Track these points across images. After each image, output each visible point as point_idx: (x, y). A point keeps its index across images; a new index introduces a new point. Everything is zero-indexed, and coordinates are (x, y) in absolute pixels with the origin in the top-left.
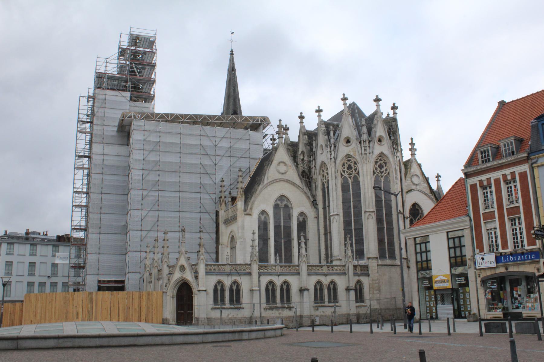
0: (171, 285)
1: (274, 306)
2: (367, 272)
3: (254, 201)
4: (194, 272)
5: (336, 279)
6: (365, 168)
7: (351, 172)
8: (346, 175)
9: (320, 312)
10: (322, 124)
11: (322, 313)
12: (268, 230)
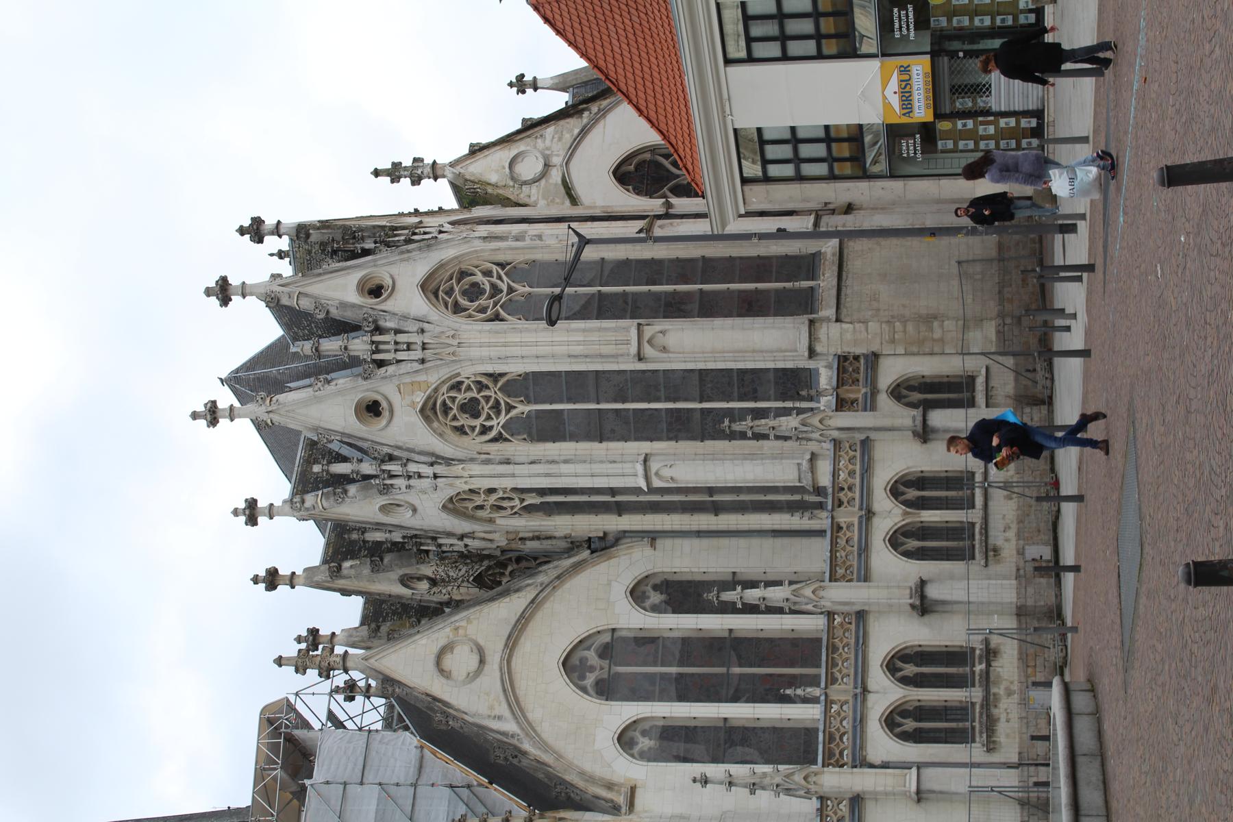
1: (981, 714)
2: (862, 361)
3: (582, 773)
5: (883, 476)
6: (475, 353)
7: (487, 402)
8: (498, 423)
9: (1007, 540)
10: (303, 502)
11: (1011, 534)
12: (693, 724)
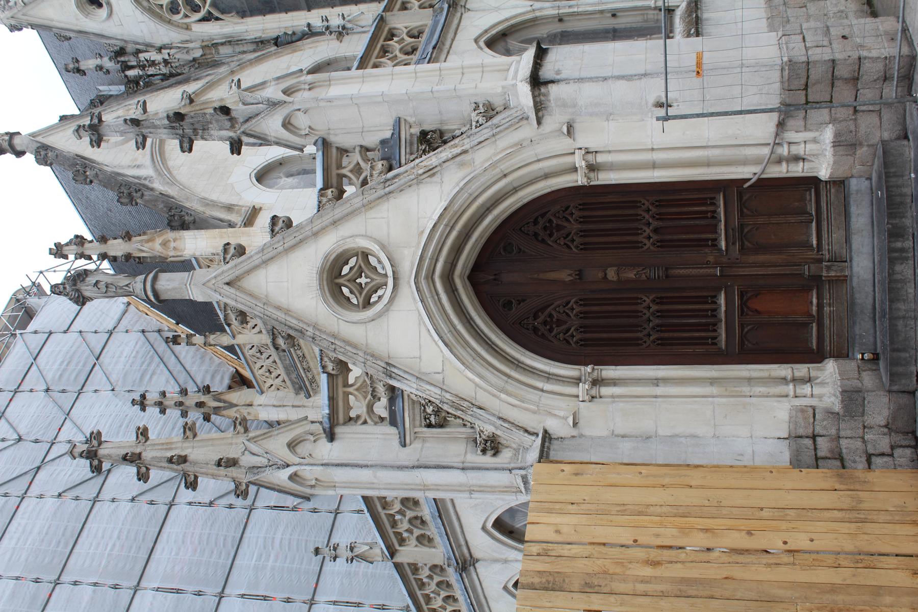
0: (483, 398)
4: (390, 169)
